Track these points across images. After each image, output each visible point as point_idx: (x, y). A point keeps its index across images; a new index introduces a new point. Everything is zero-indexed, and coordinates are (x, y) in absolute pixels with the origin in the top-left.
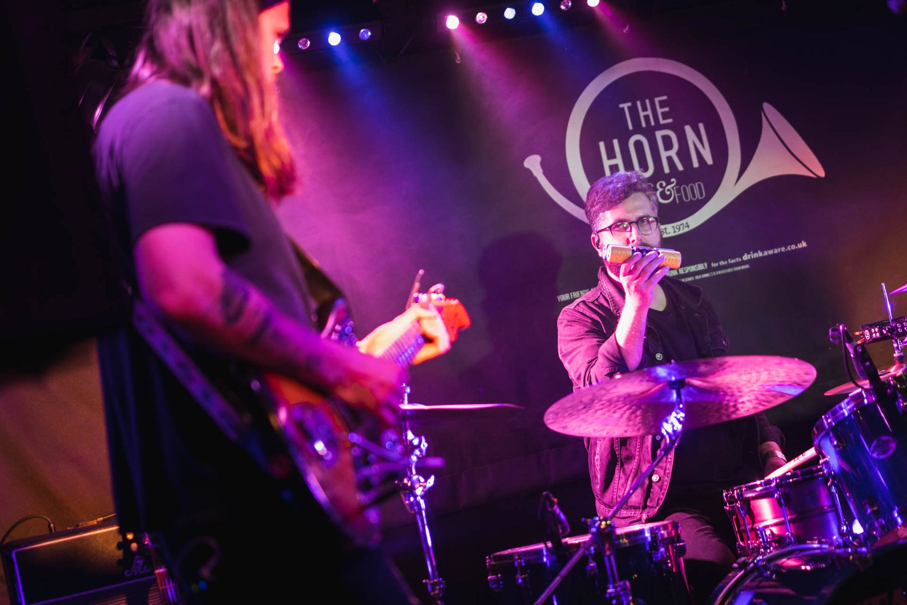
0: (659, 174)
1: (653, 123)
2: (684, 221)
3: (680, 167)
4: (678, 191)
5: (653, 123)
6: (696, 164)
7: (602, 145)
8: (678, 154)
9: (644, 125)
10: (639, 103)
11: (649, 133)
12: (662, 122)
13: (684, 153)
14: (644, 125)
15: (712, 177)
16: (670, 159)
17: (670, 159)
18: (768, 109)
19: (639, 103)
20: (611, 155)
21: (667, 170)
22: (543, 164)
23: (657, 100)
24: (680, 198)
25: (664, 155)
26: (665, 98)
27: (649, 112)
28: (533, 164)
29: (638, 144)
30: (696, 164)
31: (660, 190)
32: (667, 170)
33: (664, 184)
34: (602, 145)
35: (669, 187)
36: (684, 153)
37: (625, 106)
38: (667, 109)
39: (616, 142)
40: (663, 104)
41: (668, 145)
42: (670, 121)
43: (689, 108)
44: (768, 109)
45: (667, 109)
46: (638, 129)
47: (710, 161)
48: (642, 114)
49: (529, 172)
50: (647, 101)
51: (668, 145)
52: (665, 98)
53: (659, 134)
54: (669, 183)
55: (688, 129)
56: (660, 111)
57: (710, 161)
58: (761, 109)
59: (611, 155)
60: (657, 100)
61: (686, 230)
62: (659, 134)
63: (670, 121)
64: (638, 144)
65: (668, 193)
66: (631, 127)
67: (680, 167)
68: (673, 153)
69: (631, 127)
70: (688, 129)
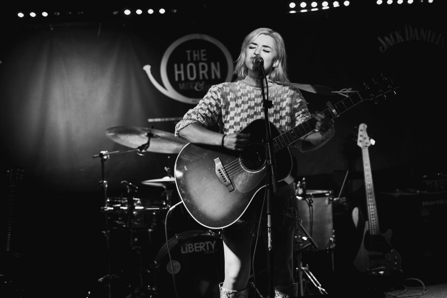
1: (199, 59)
3: (207, 77)
5: (199, 59)
6: (213, 77)
7: (176, 66)
9: (195, 59)
10: (194, 52)
12: (203, 59)
13: (209, 73)
14: (195, 59)
16: (203, 74)
17: (203, 74)
19: (194, 52)
20: (179, 69)
21: (201, 78)
22: (152, 70)
23: (202, 51)
25: (201, 72)
26: (204, 50)
27: (198, 55)
28: (147, 68)
29: (191, 68)
30: (213, 77)
32: (201, 78)
33: (199, 83)
34: (176, 66)
35: (202, 85)
36: (209, 73)
37: (188, 52)
38: (205, 55)
39: (182, 66)
40: (204, 53)
42: (205, 59)
45: (205, 55)
46: (192, 61)
48: (195, 56)
49: (145, 72)
50: (198, 52)
52: (204, 50)
53: (201, 64)
54: (201, 83)
56: (203, 55)
62: (201, 64)
63: (205, 59)
64: (191, 68)
65: (200, 87)
66: (189, 59)
67: (207, 77)
68: (205, 72)
69: (189, 59)
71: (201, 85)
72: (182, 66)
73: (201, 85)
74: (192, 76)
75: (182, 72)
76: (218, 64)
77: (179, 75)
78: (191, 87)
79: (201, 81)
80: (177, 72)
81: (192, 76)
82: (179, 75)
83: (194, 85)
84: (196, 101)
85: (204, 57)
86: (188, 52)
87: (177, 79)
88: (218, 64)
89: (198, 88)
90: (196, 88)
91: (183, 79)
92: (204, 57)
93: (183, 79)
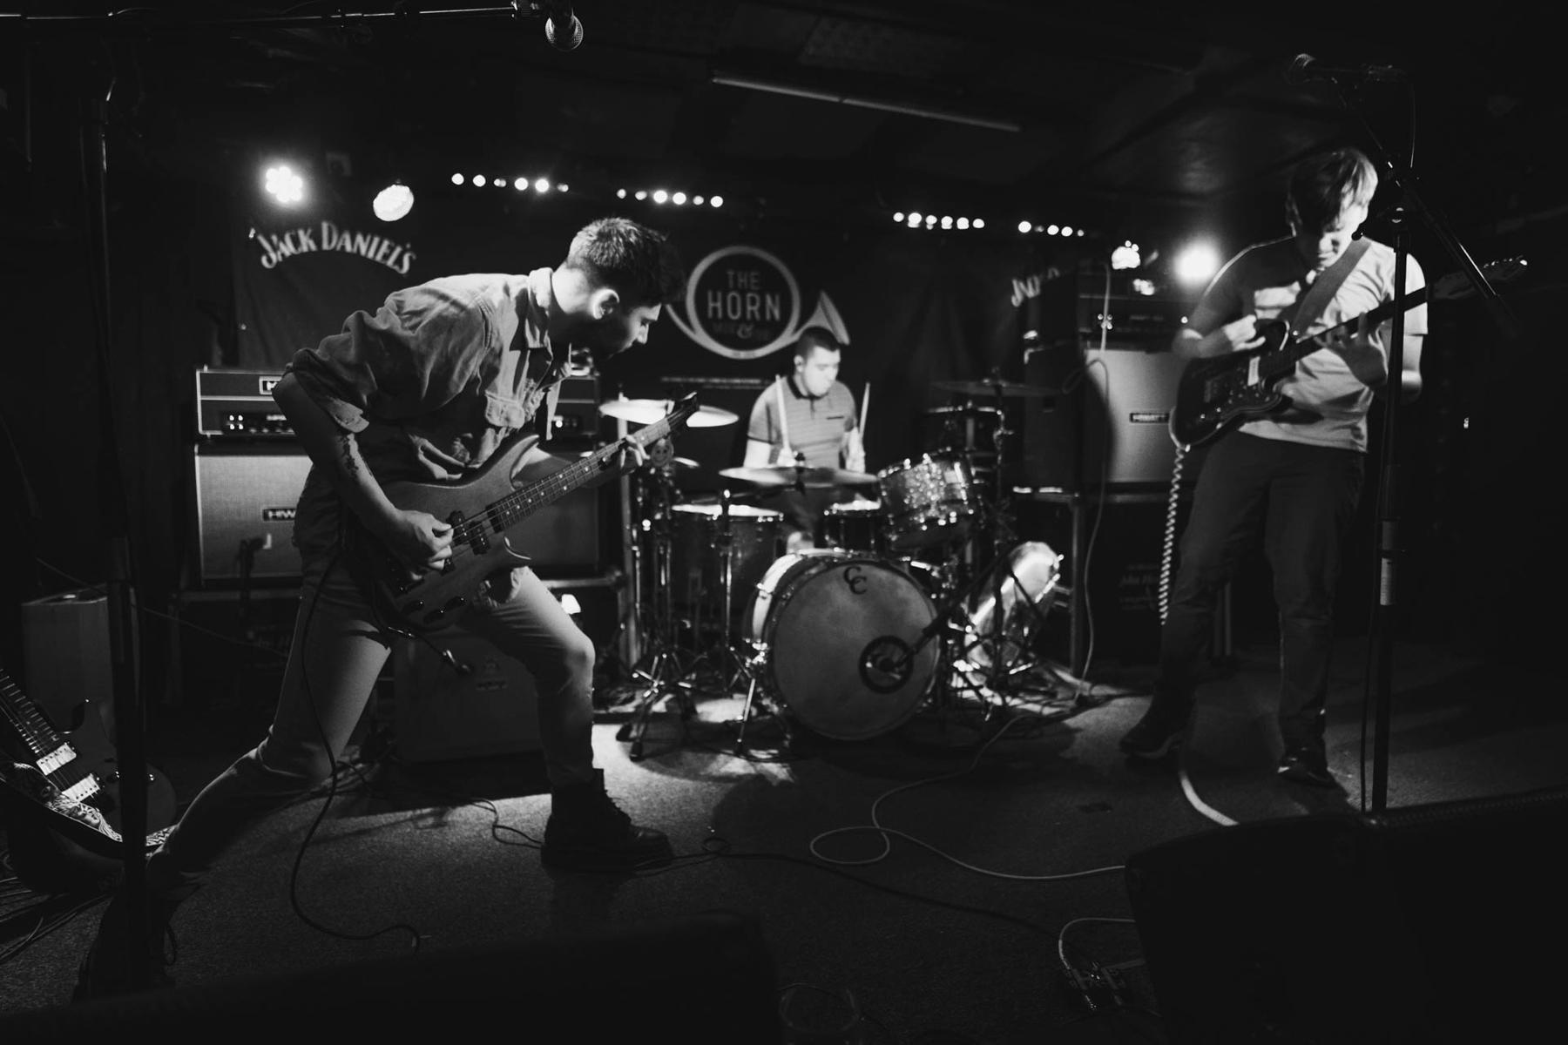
0: (743, 319)
3: (757, 316)
6: (768, 317)
11: (743, 293)
15: (776, 330)
18: (825, 298)
20: (715, 300)
21: (749, 316)
25: (749, 308)
29: (734, 299)
39: (719, 295)
43: (772, 284)
46: (736, 288)
59: (715, 300)
66: (731, 283)
67: (757, 316)
68: (755, 308)
71: (748, 329)
72: (719, 295)
73: (748, 329)
74: (734, 312)
75: (719, 305)
77: (715, 310)
79: (748, 323)
80: (711, 305)
81: (734, 312)
82: (715, 310)
83: (737, 328)
86: (731, 273)
87: (710, 314)
90: (739, 333)
91: (720, 315)
93: (720, 315)
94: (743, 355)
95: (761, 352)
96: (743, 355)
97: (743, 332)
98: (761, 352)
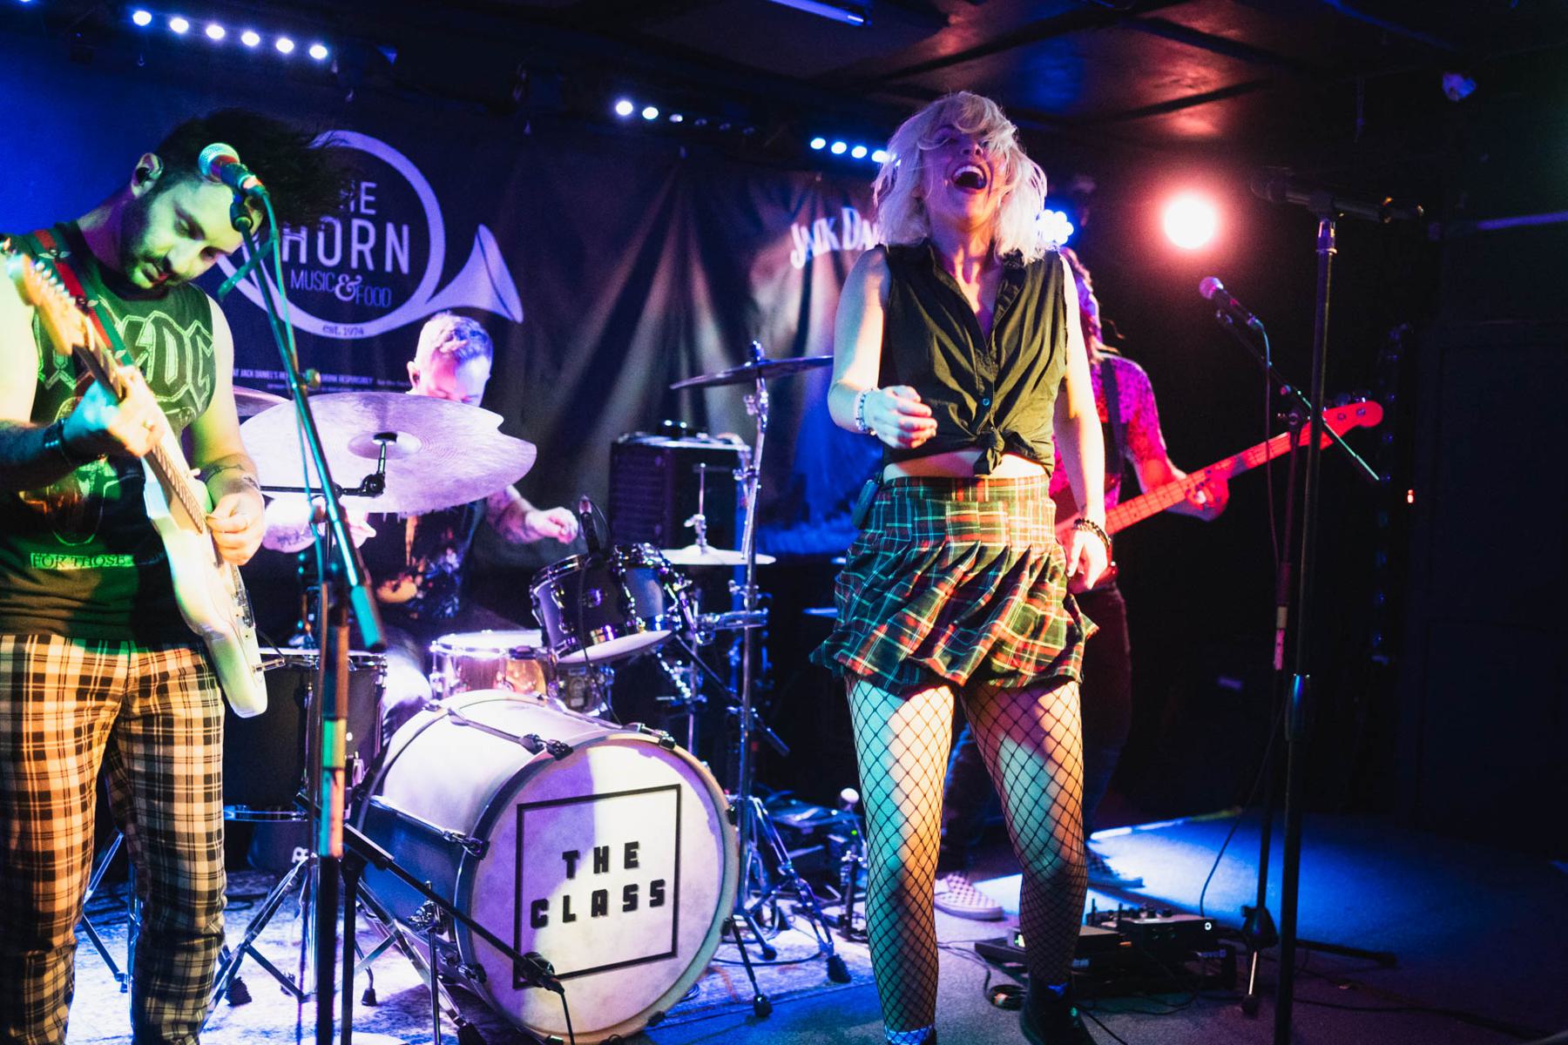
2: (359, 326)
3: (370, 266)
4: (362, 291)
6: (389, 267)
8: (372, 251)
12: (363, 210)
13: (378, 252)
15: (401, 288)
16: (361, 254)
17: (361, 254)
21: (354, 264)
23: (364, 185)
24: (361, 299)
25: (356, 246)
26: (372, 185)
30: (389, 267)
31: (341, 284)
32: (354, 264)
36: (378, 252)
38: (372, 198)
40: (369, 191)
41: (363, 238)
42: (372, 212)
43: (397, 205)
44: (483, 231)
45: (372, 198)
47: (405, 268)
51: (363, 238)
52: (372, 185)
53: (356, 223)
54: (353, 279)
55: (390, 228)
56: (364, 198)
57: (405, 268)
58: (476, 230)
60: (364, 185)
61: (359, 336)
62: (356, 223)
63: (372, 212)
67: (370, 266)
68: (366, 248)
70: (390, 228)
74: (329, 253)
76: (405, 230)
77: (294, 247)
78: (324, 286)
79: (353, 274)
81: (329, 253)
82: (294, 247)
83: (333, 283)
84: (331, 330)
85: (368, 205)
88: (405, 230)
89: (343, 290)
90: (337, 290)
91: (303, 259)
92: (368, 205)
93: (303, 259)
94: (343, 331)
95: (372, 329)
96: (343, 331)
97: (345, 290)
98: (372, 329)
